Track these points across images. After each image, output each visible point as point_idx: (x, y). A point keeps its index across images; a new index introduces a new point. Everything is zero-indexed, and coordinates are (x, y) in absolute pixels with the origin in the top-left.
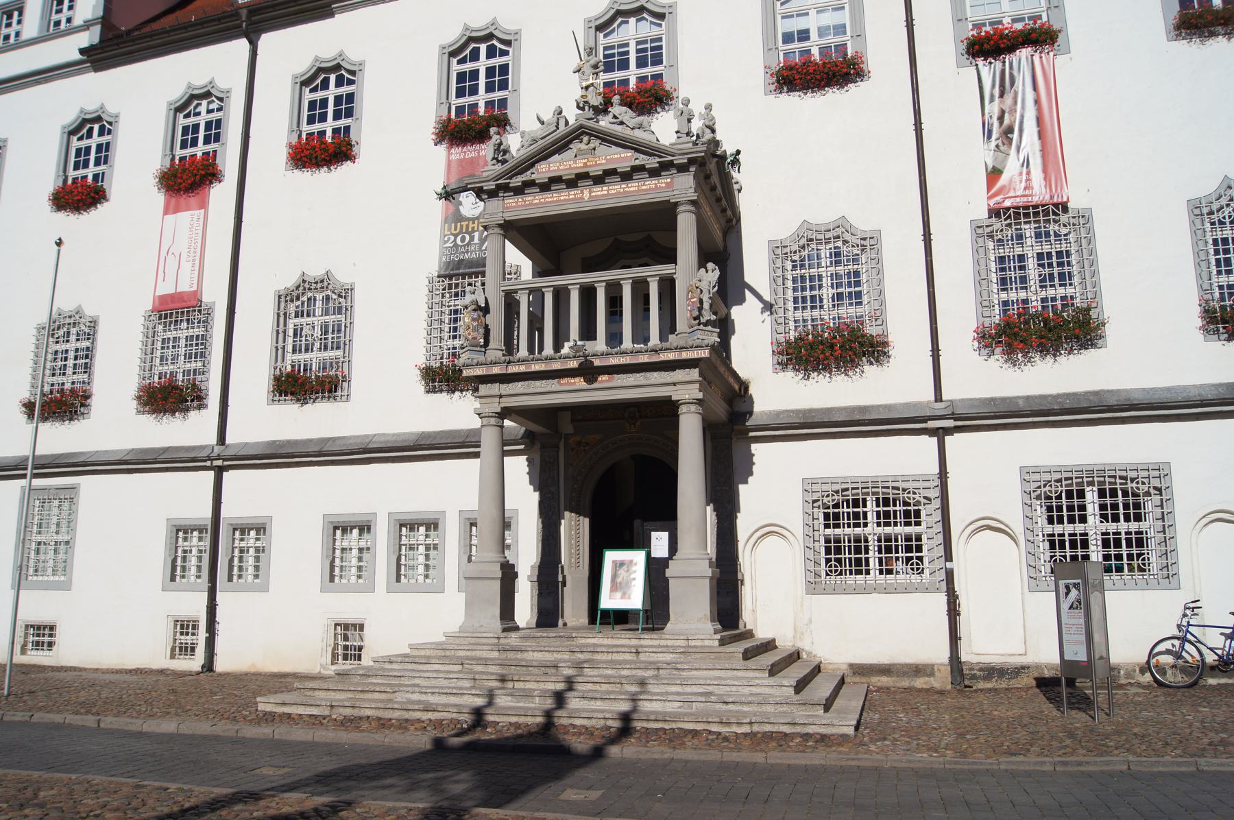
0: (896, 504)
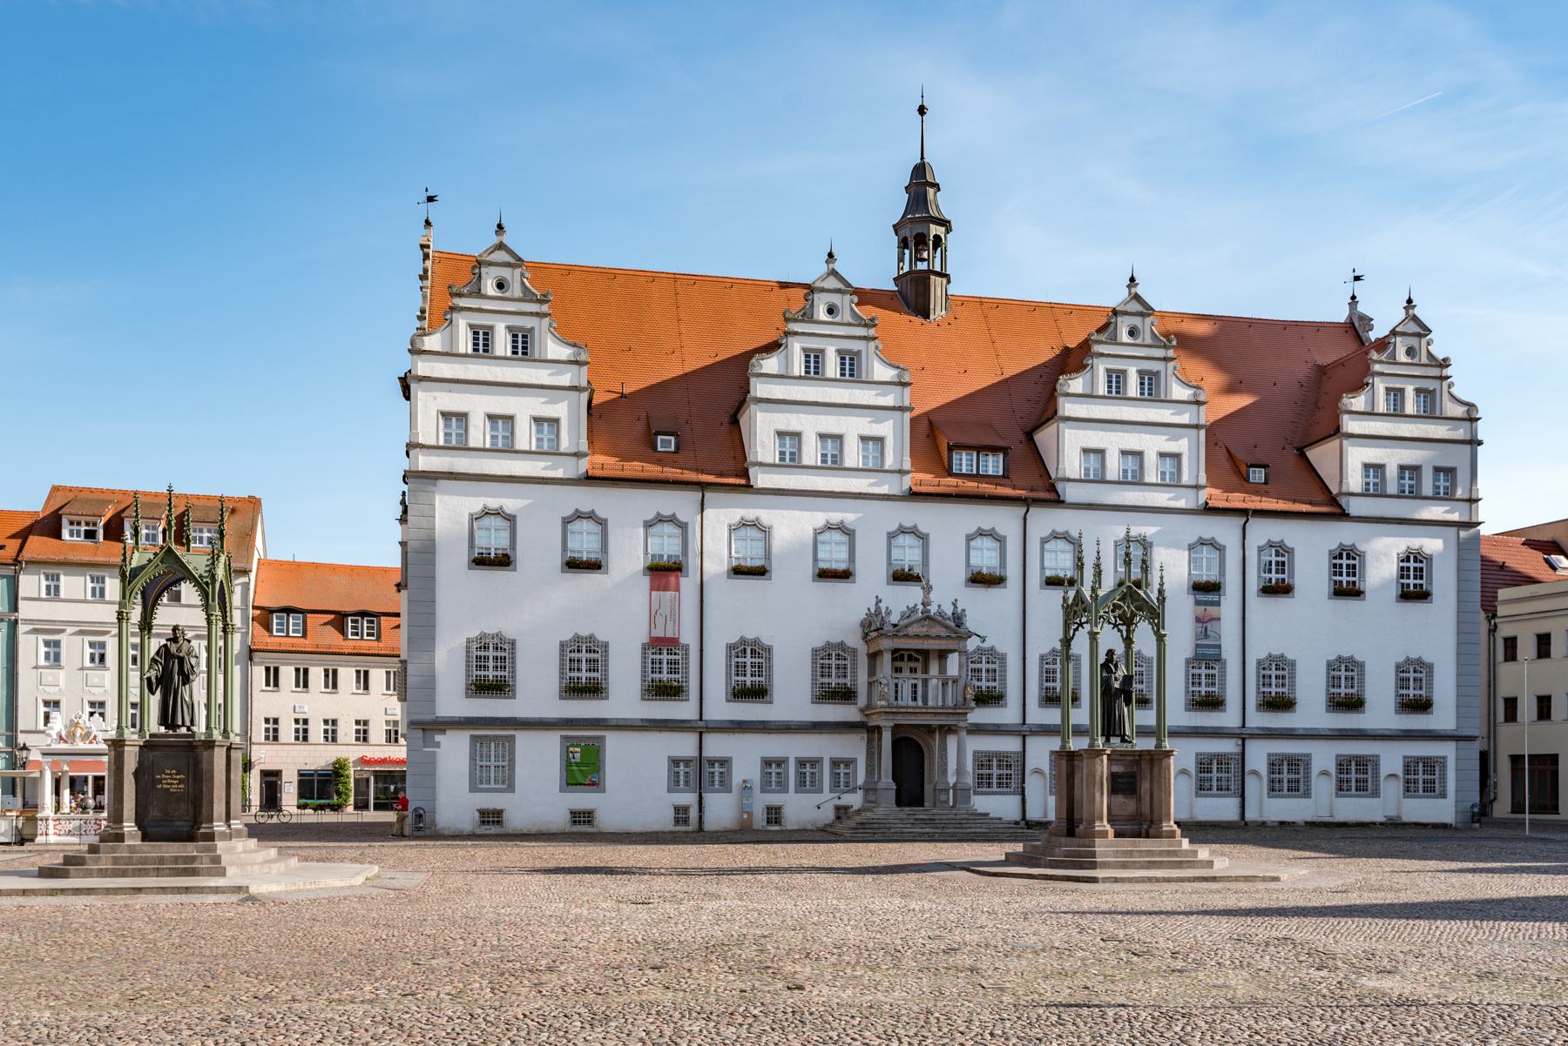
0: (1003, 759)
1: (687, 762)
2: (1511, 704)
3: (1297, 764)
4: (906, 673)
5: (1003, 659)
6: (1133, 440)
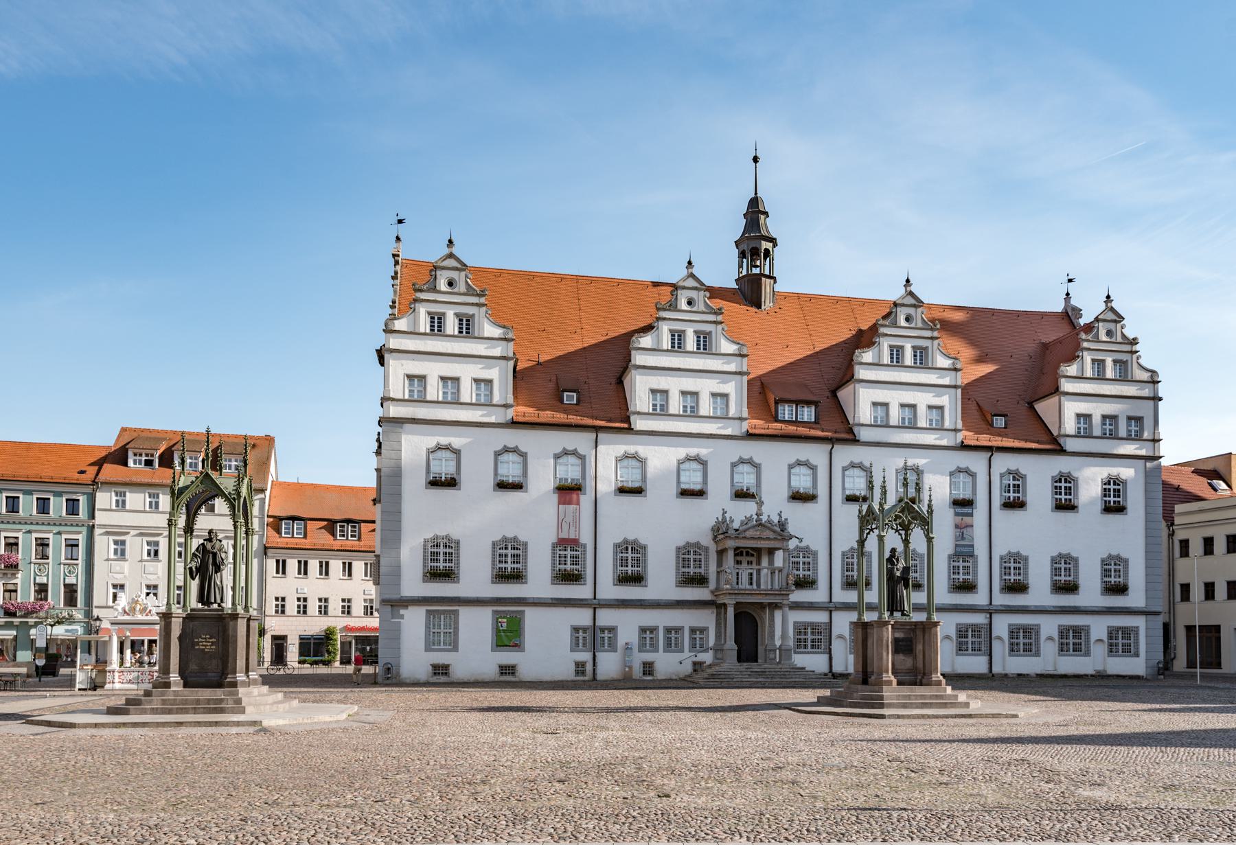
0: (815, 627)
1: (585, 629)
2: (1186, 588)
3: (1030, 632)
4: (744, 565)
5: (815, 554)
6: (909, 397)
